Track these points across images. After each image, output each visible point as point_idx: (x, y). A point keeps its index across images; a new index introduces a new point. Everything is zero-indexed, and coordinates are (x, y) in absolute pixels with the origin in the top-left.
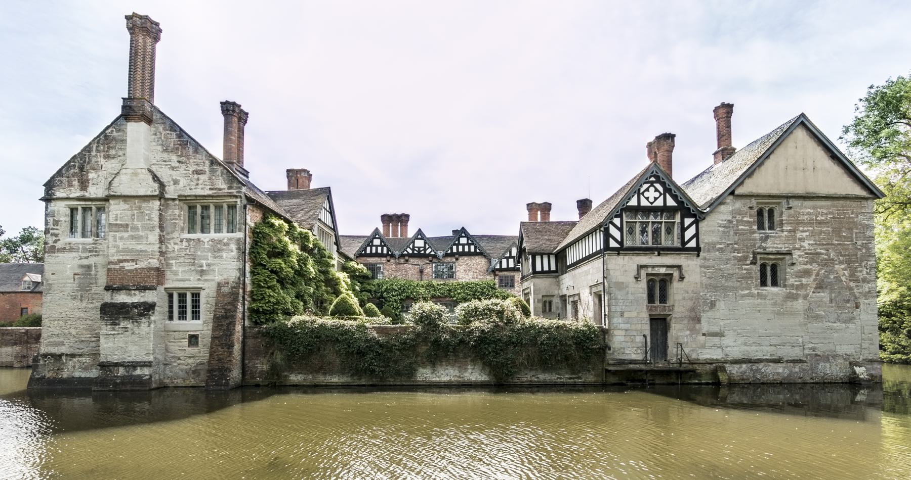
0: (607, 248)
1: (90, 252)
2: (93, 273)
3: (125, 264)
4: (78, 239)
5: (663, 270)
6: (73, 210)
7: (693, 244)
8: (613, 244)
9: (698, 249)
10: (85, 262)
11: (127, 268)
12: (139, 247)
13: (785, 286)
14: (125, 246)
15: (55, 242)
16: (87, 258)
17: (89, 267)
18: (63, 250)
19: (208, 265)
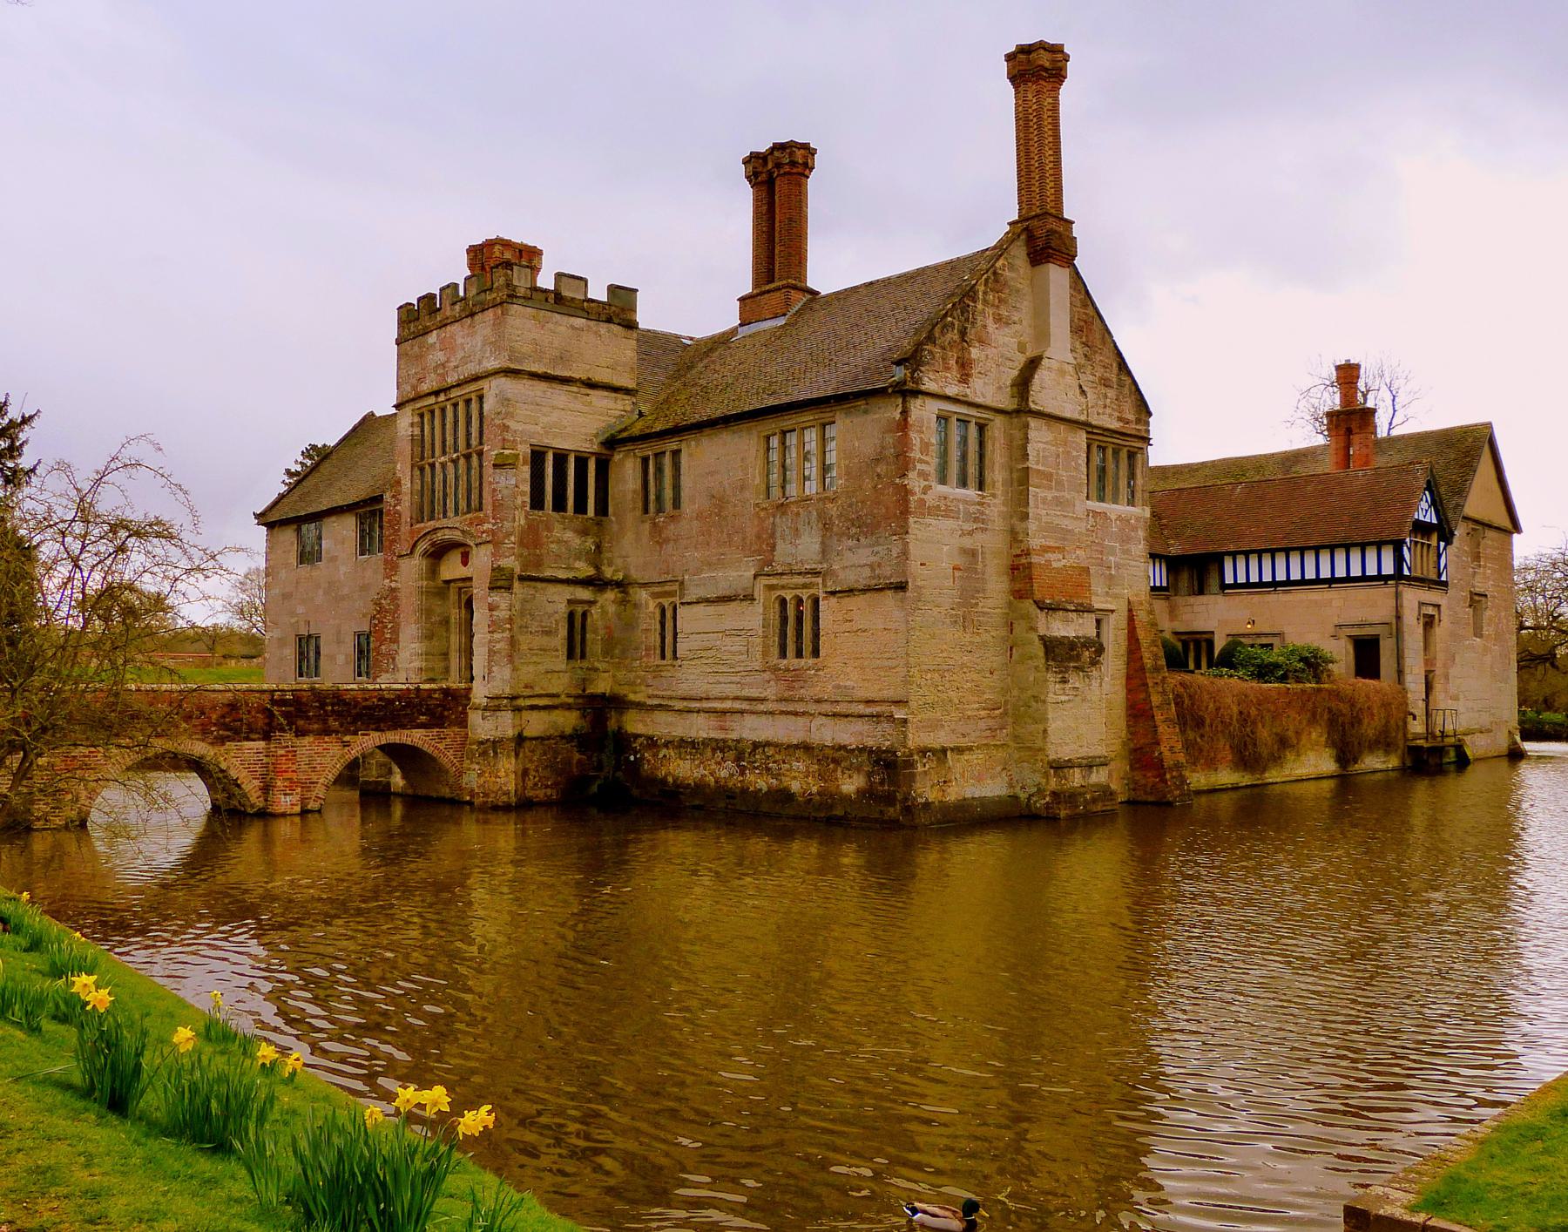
0: (1398, 576)
1: (976, 520)
2: (980, 567)
3: (1049, 556)
4: (952, 491)
5: (1430, 611)
6: (943, 418)
7: (1444, 578)
8: (1406, 572)
9: (1445, 584)
10: (968, 542)
11: (1055, 565)
12: (1066, 523)
13: (1481, 636)
14: (1048, 519)
15: (926, 490)
16: (971, 533)
17: (972, 553)
18: (934, 511)
19: (1118, 566)
